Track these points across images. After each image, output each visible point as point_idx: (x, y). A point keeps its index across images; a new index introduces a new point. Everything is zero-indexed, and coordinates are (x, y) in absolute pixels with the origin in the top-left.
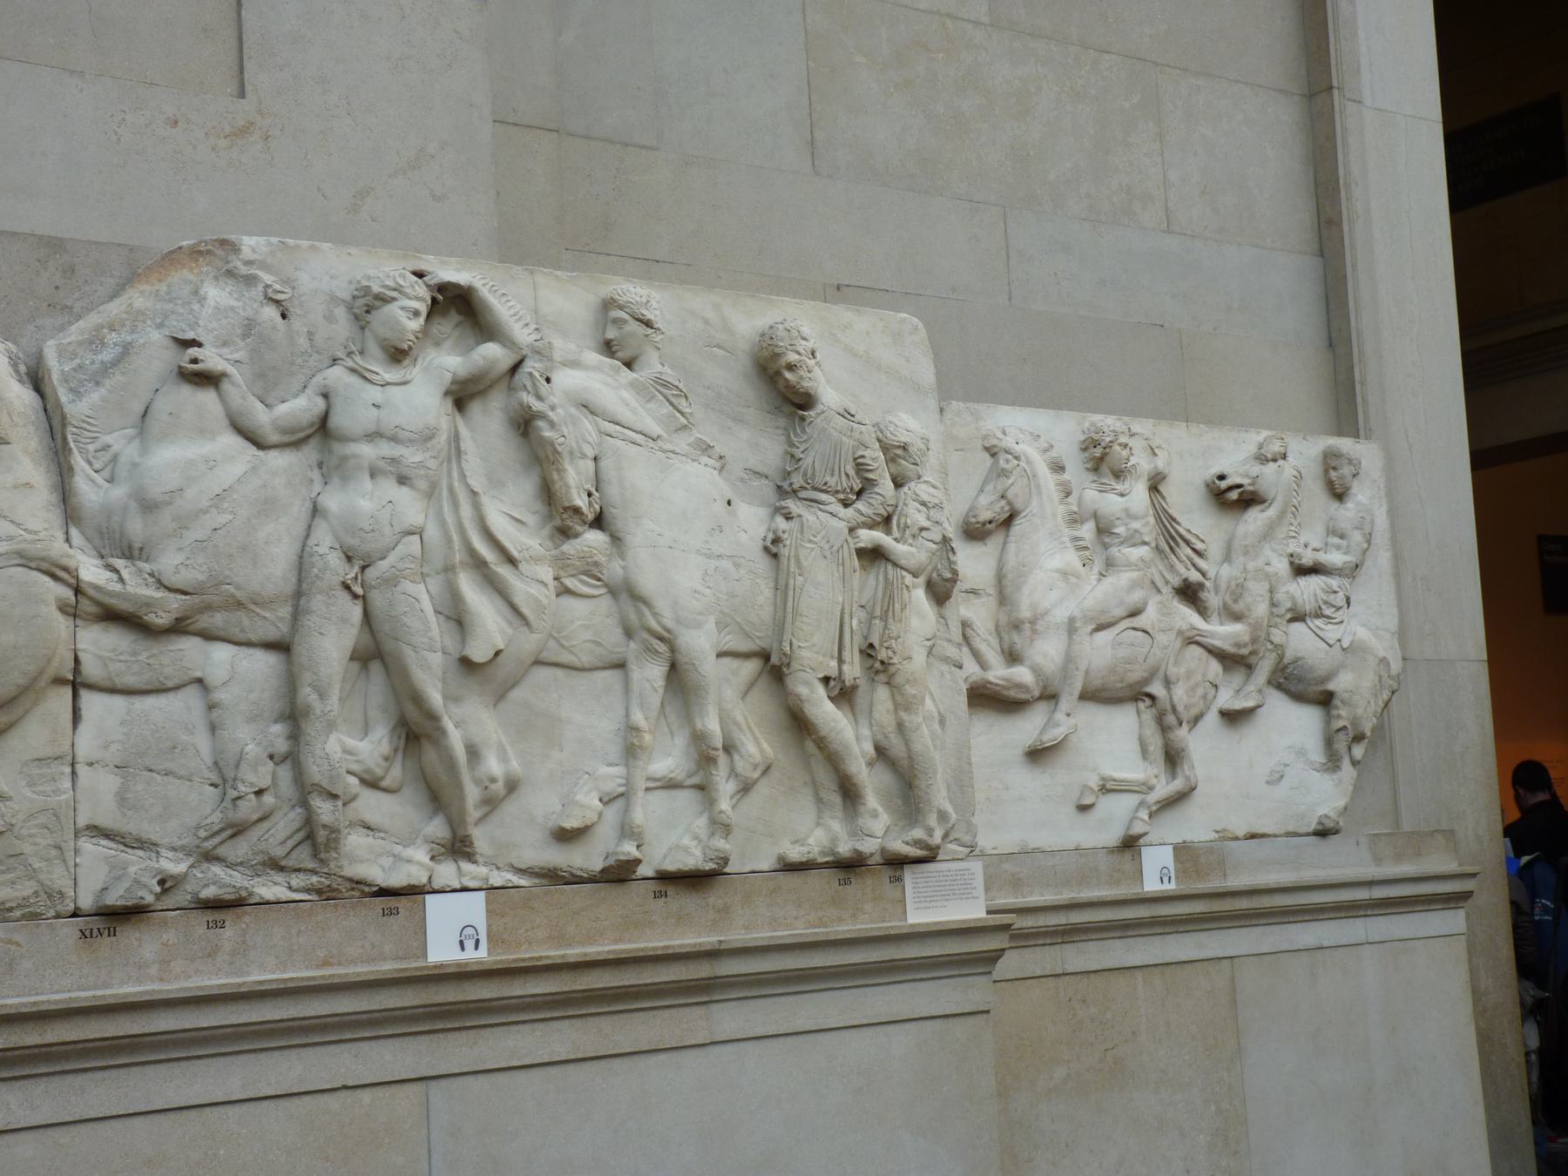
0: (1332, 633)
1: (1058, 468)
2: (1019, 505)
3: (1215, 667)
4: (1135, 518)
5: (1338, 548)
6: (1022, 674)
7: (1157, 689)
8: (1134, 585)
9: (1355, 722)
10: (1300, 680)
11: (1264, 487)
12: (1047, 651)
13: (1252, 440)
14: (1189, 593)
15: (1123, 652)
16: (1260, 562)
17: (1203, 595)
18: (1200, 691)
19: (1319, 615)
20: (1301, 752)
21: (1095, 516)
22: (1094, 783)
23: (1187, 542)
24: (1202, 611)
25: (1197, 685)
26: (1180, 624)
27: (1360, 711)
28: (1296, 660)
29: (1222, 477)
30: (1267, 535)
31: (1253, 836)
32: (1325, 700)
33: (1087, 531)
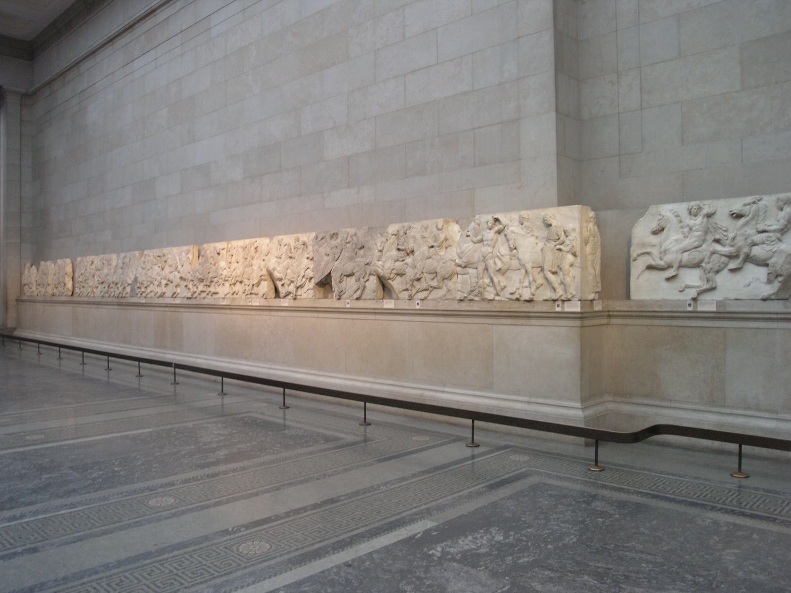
0: (768, 248)
1: (678, 216)
2: (664, 226)
3: (724, 259)
4: (697, 225)
5: (776, 224)
6: (662, 263)
7: (703, 265)
8: (695, 242)
9: (775, 271)
10: (756, 261)
11: (743, 212)
12: (669, 258)
13: (749, 199)
14: (717, 241)
15: (691, 257)
16: (742, 232)
17: (721, 242)
18: (717, 265)
19: (763, 243)
20: (758, 279)
21: (688, 226)
22: (683, 285)
23: (721, 229)
24: (724, 245)
25: (716, 264)
26: (711, 249)
27: (777, 268)
28: (754, 256)
29: (731, 211)
30: (746, 224)
31: (737, 299)
32: (767, 265)
33: (686, 230)
